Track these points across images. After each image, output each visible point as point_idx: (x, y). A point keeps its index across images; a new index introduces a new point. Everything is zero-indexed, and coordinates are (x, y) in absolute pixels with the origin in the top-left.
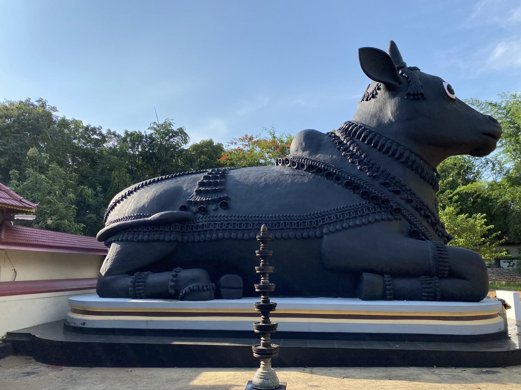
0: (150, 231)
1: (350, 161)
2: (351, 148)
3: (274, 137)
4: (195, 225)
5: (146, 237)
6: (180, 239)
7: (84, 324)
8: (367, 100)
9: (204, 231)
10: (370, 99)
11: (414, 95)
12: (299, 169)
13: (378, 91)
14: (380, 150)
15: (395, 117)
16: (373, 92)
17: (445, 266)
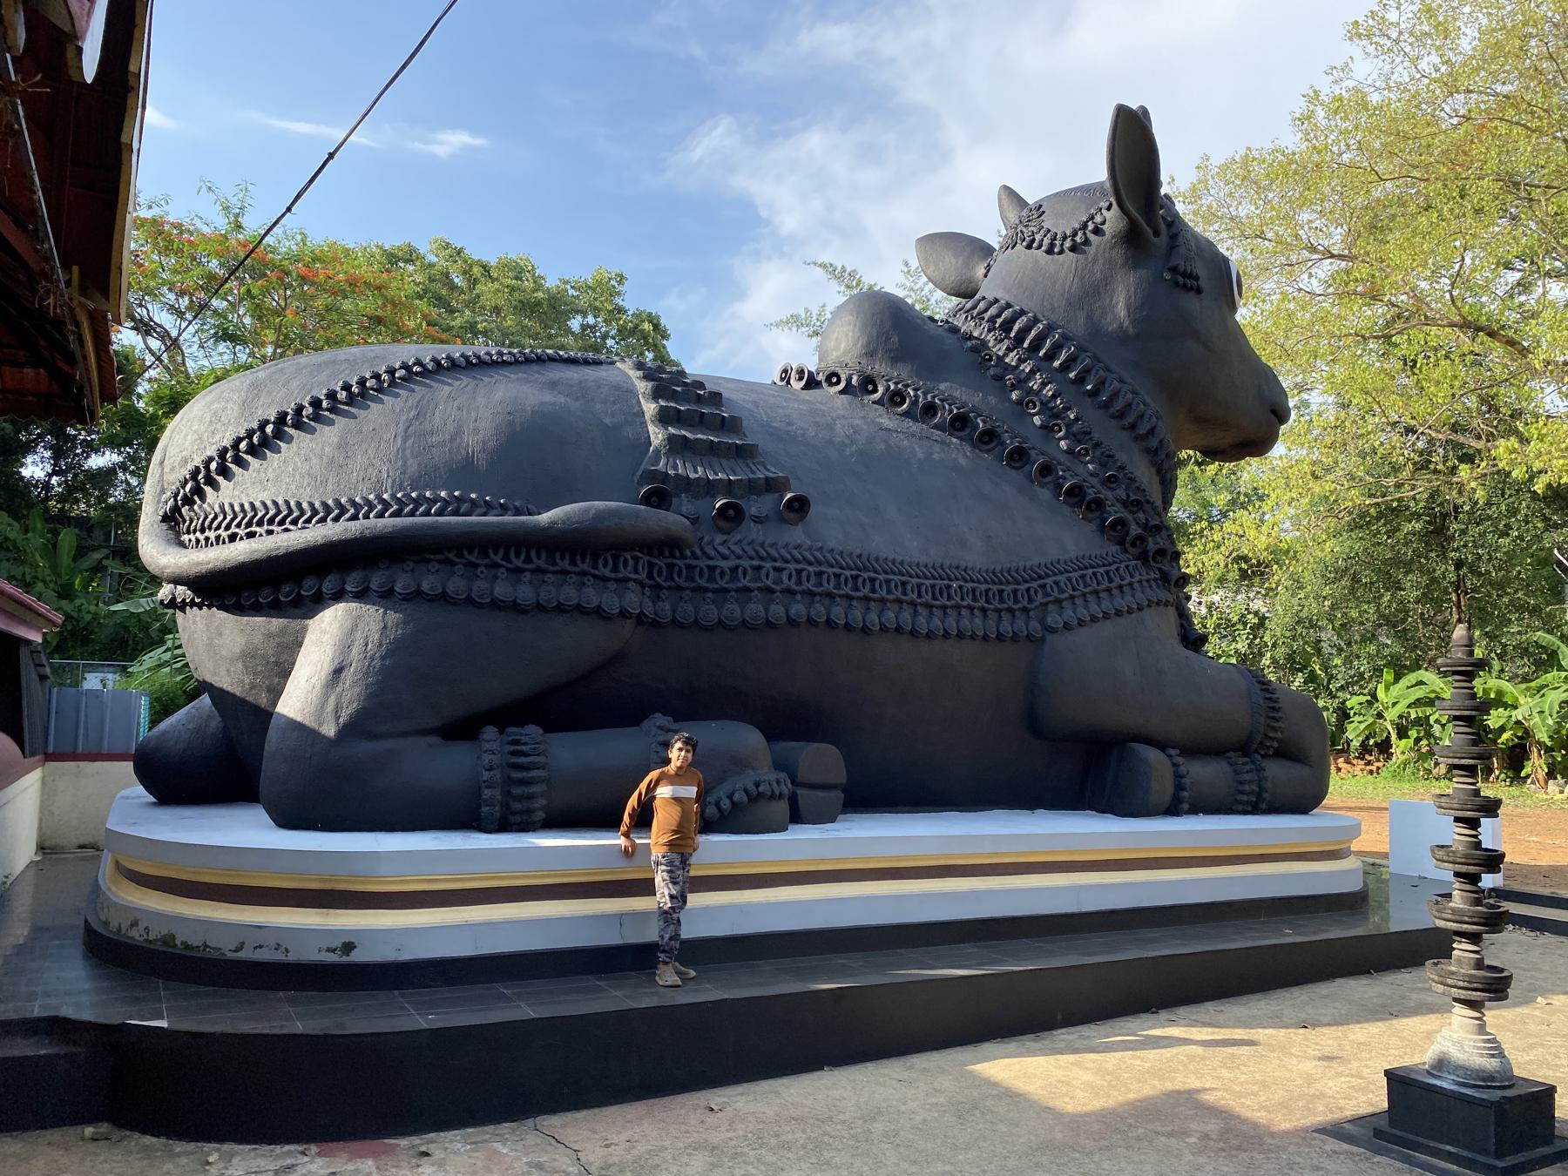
0: (539, 571)
1: (1037, 420)
2: (1034, 385)
3: (239, 227)
4: (703, 563)
5: (525, 593)
6: (649, 610)
7: (348, 947)
8: (1050, 251)
9: (738, 590)
10: (1061, 252)
11: (1184, 275)
12: (915, 419)
13: (1092, 237)
14: (1105, 406)
15: (1134, 321)
16: (1075, 234)
17: (1275, 729)
